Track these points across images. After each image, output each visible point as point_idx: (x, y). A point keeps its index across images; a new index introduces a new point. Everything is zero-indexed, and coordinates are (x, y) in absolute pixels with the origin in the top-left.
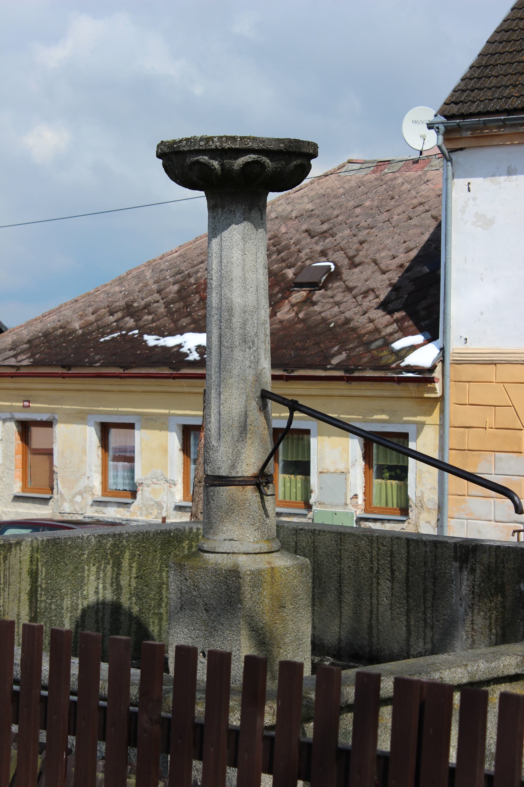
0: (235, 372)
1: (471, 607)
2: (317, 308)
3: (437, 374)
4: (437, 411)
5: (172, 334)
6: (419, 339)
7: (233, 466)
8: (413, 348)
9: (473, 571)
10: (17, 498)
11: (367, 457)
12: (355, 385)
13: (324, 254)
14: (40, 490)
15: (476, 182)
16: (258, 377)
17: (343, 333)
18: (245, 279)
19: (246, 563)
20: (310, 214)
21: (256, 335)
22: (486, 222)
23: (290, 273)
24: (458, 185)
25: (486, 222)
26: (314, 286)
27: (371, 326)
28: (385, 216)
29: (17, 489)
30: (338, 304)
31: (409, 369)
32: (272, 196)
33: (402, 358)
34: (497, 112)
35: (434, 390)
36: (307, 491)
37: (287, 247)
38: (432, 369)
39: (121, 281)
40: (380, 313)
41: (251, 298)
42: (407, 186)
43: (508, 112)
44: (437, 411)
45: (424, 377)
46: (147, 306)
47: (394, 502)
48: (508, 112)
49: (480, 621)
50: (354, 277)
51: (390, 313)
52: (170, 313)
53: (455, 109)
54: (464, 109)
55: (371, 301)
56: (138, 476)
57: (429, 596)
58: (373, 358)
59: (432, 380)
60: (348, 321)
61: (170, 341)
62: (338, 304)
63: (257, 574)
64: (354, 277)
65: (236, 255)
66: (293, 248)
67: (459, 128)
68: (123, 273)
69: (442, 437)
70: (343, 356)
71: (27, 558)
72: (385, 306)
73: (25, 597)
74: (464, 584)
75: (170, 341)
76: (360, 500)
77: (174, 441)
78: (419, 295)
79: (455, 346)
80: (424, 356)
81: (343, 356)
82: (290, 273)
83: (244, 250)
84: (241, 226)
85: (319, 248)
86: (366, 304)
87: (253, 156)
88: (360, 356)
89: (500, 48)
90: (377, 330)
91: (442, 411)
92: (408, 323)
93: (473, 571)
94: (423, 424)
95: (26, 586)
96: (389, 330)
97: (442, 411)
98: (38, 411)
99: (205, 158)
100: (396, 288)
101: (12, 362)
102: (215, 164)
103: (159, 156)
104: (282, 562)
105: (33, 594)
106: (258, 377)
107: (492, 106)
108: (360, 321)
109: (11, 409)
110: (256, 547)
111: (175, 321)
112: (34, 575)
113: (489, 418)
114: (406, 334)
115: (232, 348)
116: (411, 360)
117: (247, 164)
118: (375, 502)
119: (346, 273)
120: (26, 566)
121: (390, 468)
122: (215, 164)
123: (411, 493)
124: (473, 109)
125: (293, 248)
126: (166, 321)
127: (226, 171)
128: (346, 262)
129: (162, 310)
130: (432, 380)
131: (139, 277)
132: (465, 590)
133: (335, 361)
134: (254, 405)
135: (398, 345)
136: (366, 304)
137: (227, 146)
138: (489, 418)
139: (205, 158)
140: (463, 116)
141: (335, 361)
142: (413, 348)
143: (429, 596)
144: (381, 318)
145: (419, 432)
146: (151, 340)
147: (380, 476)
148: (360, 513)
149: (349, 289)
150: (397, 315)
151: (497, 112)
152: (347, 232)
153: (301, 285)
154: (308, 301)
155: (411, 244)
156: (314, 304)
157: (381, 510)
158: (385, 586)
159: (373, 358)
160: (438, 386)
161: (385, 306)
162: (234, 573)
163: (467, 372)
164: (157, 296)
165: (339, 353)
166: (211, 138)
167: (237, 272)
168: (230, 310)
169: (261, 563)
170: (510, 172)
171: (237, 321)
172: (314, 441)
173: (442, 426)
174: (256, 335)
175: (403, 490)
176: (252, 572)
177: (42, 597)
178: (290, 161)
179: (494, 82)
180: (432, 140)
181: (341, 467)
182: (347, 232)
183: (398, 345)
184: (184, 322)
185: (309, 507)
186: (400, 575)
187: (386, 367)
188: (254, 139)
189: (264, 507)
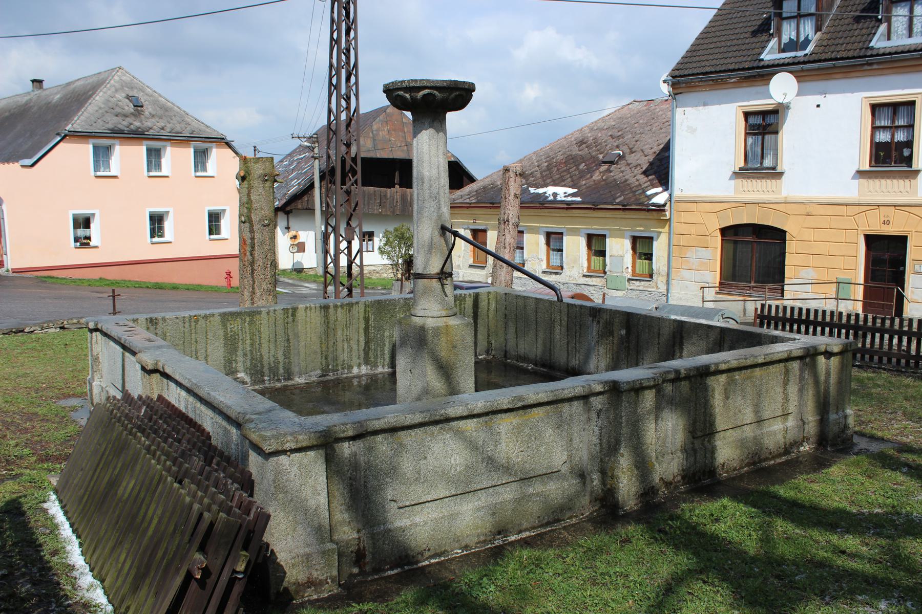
0: (426, 214)
1: (598, 342)
2: (612, 174)
3: (667, 207)
4: (667, 226)
5: (542, 187)
6: (660, 189)
7: (425, 268)
8: (657, 194)
9: (598, 322)
10: (471, 266)
11: (634, 248)
12: (627, 212)
13: (618, 147)
14: (482, 263)
15: (688, 110)
16: (440, 217)
17: (624, 186)
18: (430, 161)
19: (430, 323)
20: (613, 127)
21: (438, 193)
22: (692, 130)
23: (601, 156)
24: (679, 111)
25: (692, 130)
26: (611, 163)
27: (637, 183)
28: (649, 128)
29: (471, 262)
30: (622, 172)
31: (653, 205)
32: (449, 115)
33: (650, 199)
34: (698, 74)
35: (665, 215)
36: (605, 265)
37: (601, 144)
38: (664, 205)
39: (521, 161)
40: (643, 176)
41: (434, 172)
42: (661, 113)
43: (703, 74)
44: (667, 226)
45: (660, 208)
46: (531, 174)
47: (646, 272)
48: (703, 74)
49: (602, 350)
50: (631, 158)
51: (647, 176)
52: (542, 177)
53: (677, 73)
54: (682, 73)
55: (639, 170)
56: (525, 257)
57: (578, 334)
58: (636, 199)
59: (664, 210)
60: (626, 180)
61: (541, 191)
62: (622, 172)
63: (437, 330)
64: (631, 158)
65: (425, 148)
66: (604, 144)
67: (679, 83)
68: (522, 157)
69: (669, 239)
70: (622, 198)
71: (362, 310)
72: (645, 173)
73: (362, 331)
74: (594, 330)
75: (541, 191)
76: (630, 270)
77: (542, 239)
78: (660, 169)
79: (677, 193)
80: (661, 199)
81: (622, 198)
82: (601, 156)
83: (429, 145)
84: (428, 131)
85: (616, 144)
86: (636, 172)
87: (426, 91)
88: (630, 198)
89: (702, 42)
90: (640, 185)
91: (670, 226)
92: (656, 181)
93: (598, 322)
94: (660, 232)
95: (362, 325)
96: (646, 185)
97: (670, 226)
98: (480, 224)
99: (401, 93)
100: (651, 164)
101: (468, 201)
102: (408, 96)
103: (384, 92)
104: (453, 322)
105: (366, 329)
106: (440, 217)
107: (695, 71)
108: (632, 181)
109: (468, 224)
110: (439, 314)
111: (544, 181)
112: (367, 320)
113: (693, 230)
114: (654, 186)
115: (424, 201)
116: (655, 200)
117: (425, 95)
118: (637, 271)
119: (627, 156)
120: (362, 315)
121: (645, 254)
122: (408, 96)
123: (654, 267)
124: (686, 72)
125: (604, 144)
126: (540, 181)
127: (414, 99)
128: (628, 151)
129: (539, 175)
130: (664, 210)
131: (530, 159)
132: (595, 333)
133: (617, 201)
134: (437, 233)
135: (649, 193)
136: (636, 172)
137: (412, 85)
138: (693, 230)
139: (401, 93)
140: (681, 76)
141: (617, 201)
142: (657, 194)
143: (578, 334)
144: (643, 179)
145: (658, 237)
146: (532, 190)
147: (640, 258)
148: (629, 276)
149: (628, 164)
150: (650, 177)
151: (698, 74)
152: (630, 136)
153: (605, 162)
154: (608, 171)
155: (660, 142)
156: (611, 172)
157: (641, 275)
158: (557, 328)
159: (636, 199)
160: (668, 213)
161: (645, 173)
162: (422, 329)
163: (683, 206)
164: (537, 169)
165: (620, 196)
166: (404, 81)
167: (426, 158)
168: (422, 179)
169: (441, 322)
170: (705, 105)
171: (426, 185)
172: (607, 240)
173: (669, 233)
174: (438, 193)
175: (651, 265)
176: (433, 328)
177: (372, 331)
178: (458, 95)
179: (697, 59)
180: (665, 89)
181: (621, 254)
182: (630, 136)
183: (649, 193)
184: (548, 181)
185: (605, 273)
186: (564, 323)
187: (642, 204)
188: (428, 81)
189: (444, 291)
